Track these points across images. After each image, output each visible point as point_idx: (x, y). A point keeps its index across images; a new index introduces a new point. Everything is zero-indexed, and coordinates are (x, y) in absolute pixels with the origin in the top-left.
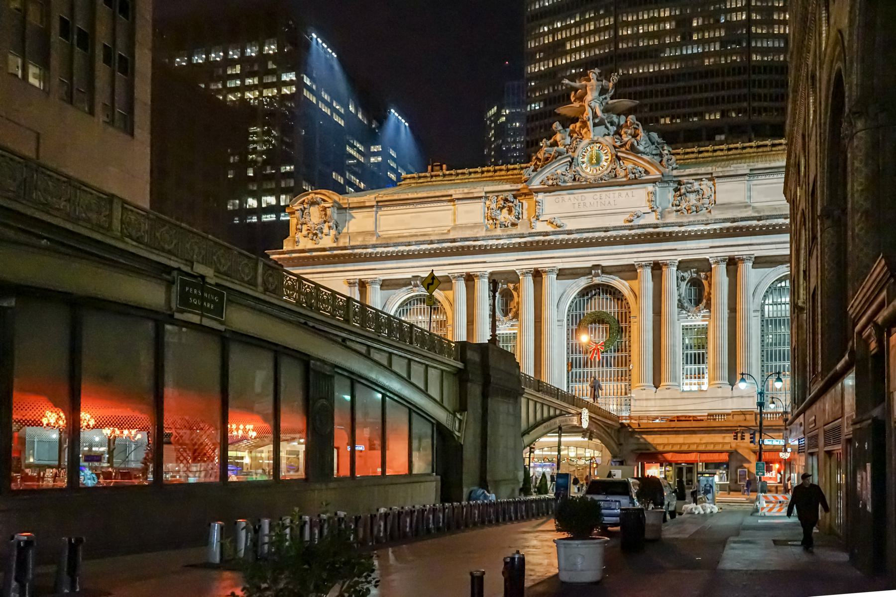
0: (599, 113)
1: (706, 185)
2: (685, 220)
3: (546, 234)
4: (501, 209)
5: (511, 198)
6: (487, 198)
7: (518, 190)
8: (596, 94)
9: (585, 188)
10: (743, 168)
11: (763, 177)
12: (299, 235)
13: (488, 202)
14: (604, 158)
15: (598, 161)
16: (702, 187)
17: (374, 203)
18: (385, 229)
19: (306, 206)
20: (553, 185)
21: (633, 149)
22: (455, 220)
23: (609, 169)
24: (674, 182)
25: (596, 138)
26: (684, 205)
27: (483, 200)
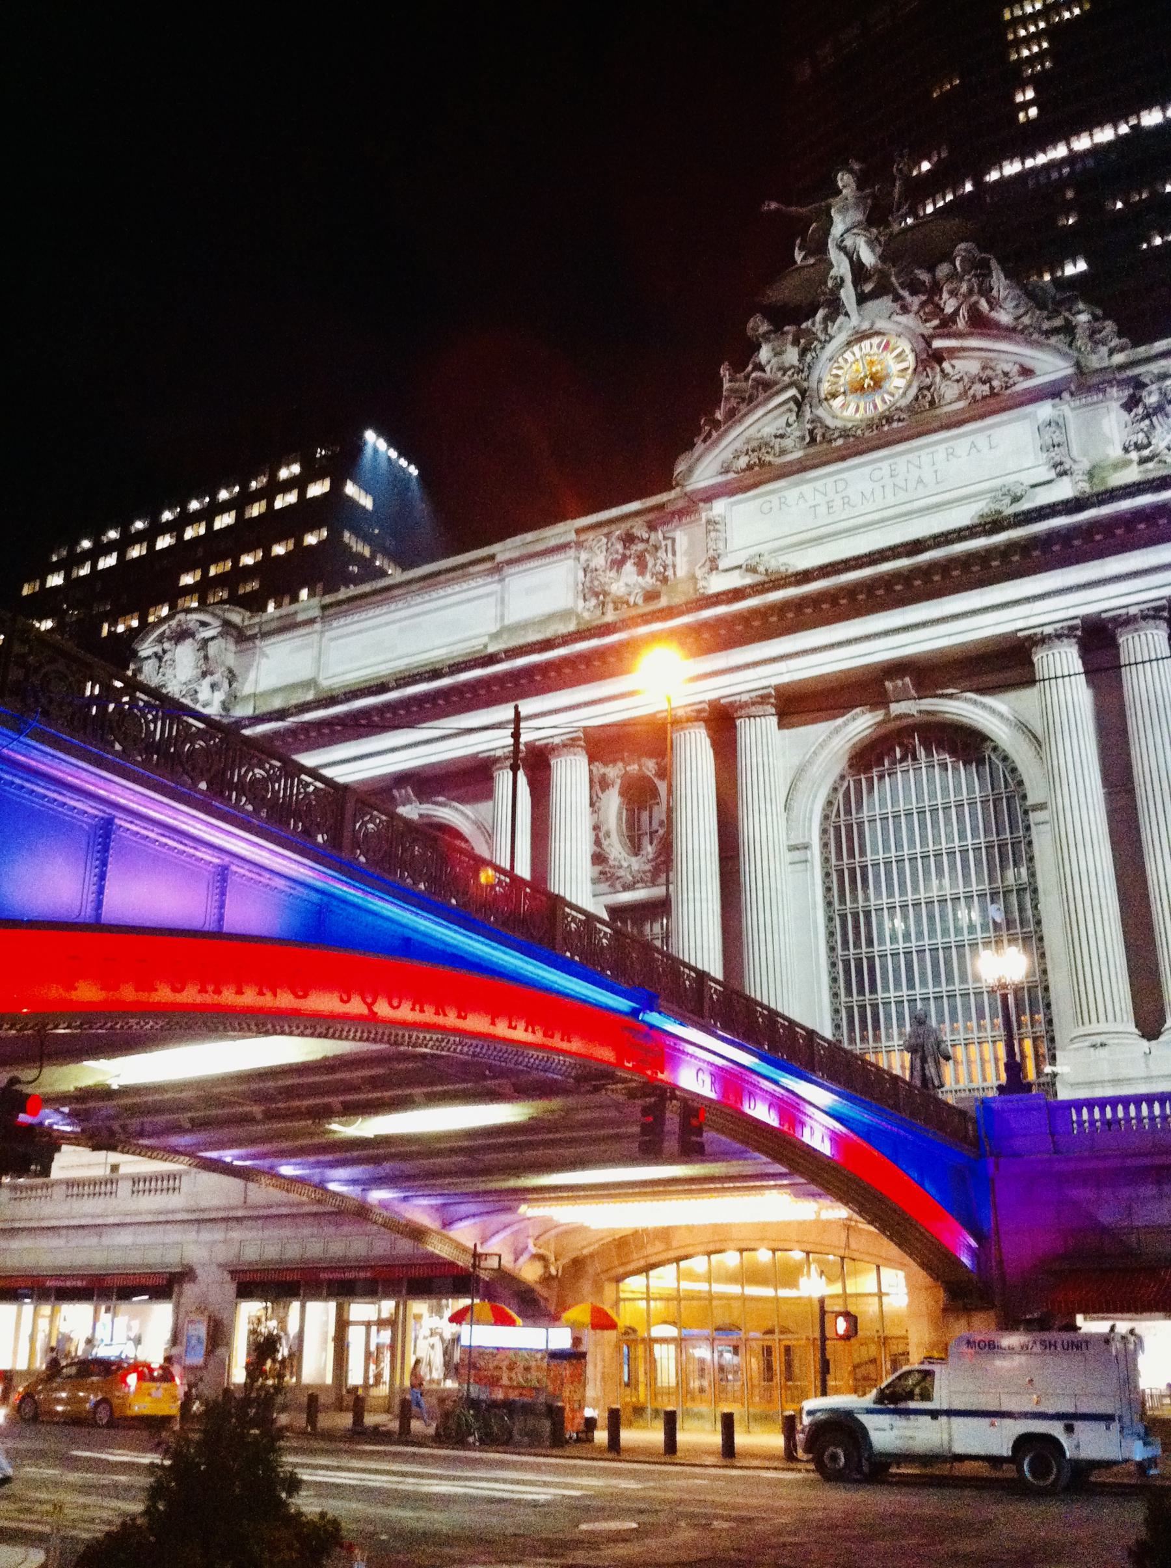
0: (868, 258)
3: (737, 594)
4: (618, 564)
5: (640, 531)
6: (579, 545)
7: (661, 507)
8: (857, 216)
9: (843, 458)
13: (584, 556)
18: (339, 670)
19: (167, 645)
20: (750, 467)
21: (980, 324)
22: (502, 617)
23: (913, 391)
24: (1121, 383)
25: (865, 326)
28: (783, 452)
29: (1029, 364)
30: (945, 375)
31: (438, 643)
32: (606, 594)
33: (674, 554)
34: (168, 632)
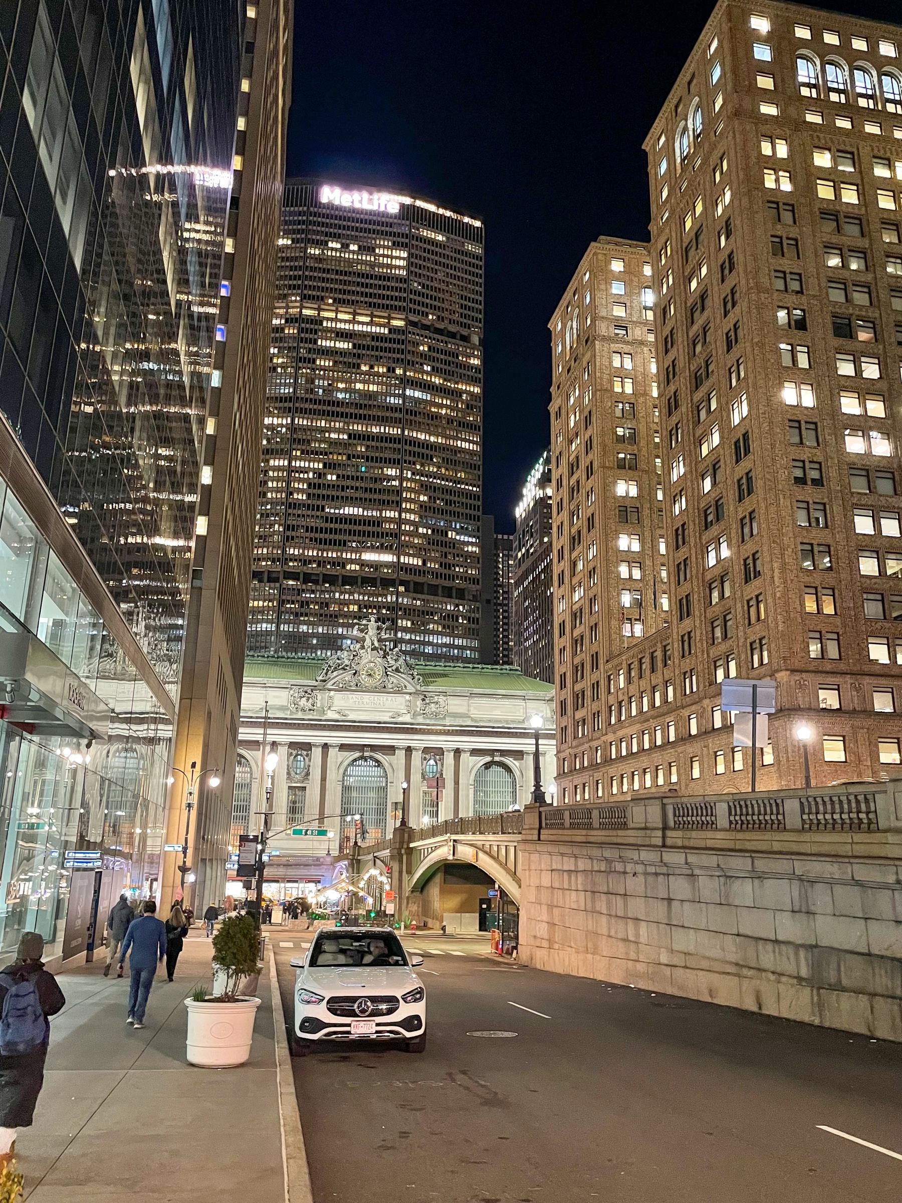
2: (428, 722)
4: (301, 697)
5: (309, 691)
10: (466, 690)
29: (407, 684)
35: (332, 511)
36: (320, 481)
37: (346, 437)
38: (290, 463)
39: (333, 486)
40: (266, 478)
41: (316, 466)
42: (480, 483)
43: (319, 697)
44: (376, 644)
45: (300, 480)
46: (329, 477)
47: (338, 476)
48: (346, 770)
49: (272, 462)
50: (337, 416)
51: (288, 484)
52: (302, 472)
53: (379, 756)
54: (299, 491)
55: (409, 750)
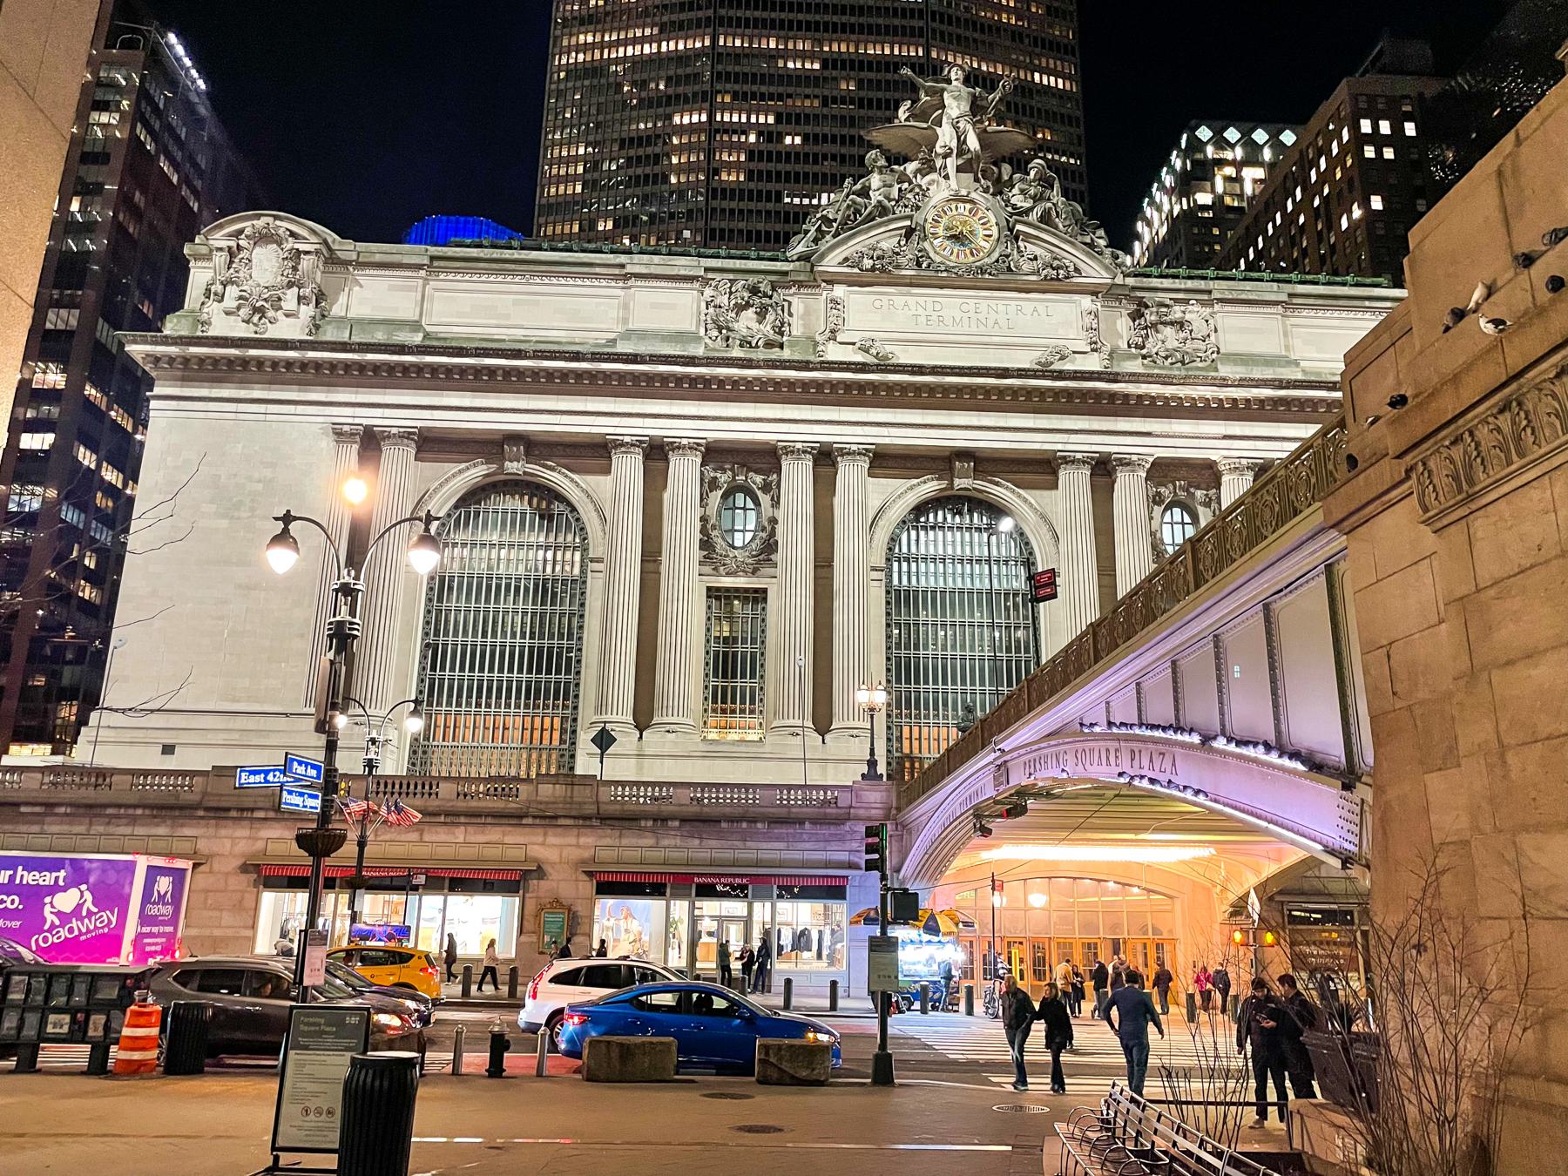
1: (1195, 314)
4: (740, 308)
5: (762, 287)
7: (786, 273)
11: (1312, 313)
12: (213, 308)
14: (981, 232)
15: (957, 238)
16: (1188, 317)
17: (426, 261)
20: (873, 269)
22: (625, 321)
23: (996, 255)
25: (964, 192)
26: (1152, 346)
27: (696, 285)
28: (898, 267)
29: (1081, 265)
30: (1019, 251)
31: (555, 324)
32: (729, 329)
33: (790, 315)
34: (248, 231)
35: (797, 201)
36: (771, 147)
37: (817, 66)
38: (711, 117)
39: (797, 154)
40: (667, 148)
41: (762, 120)
42: (1082, 150)
43: (798, 303)
44: (973, 143)
45: (731, 148)
46: (788, 140)
47: (805, 138)
48: (894, 539)
49: (677, 120)
50: (799, 29)
51: (710, 154)
52: (735, 132)
53: (1001, 491)
54: (729, 166)
55: (1103, 469)
